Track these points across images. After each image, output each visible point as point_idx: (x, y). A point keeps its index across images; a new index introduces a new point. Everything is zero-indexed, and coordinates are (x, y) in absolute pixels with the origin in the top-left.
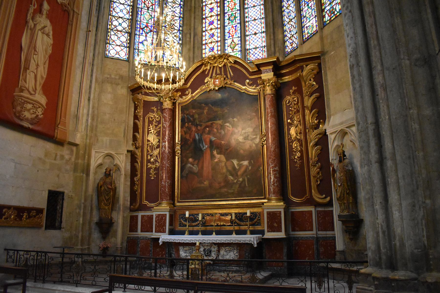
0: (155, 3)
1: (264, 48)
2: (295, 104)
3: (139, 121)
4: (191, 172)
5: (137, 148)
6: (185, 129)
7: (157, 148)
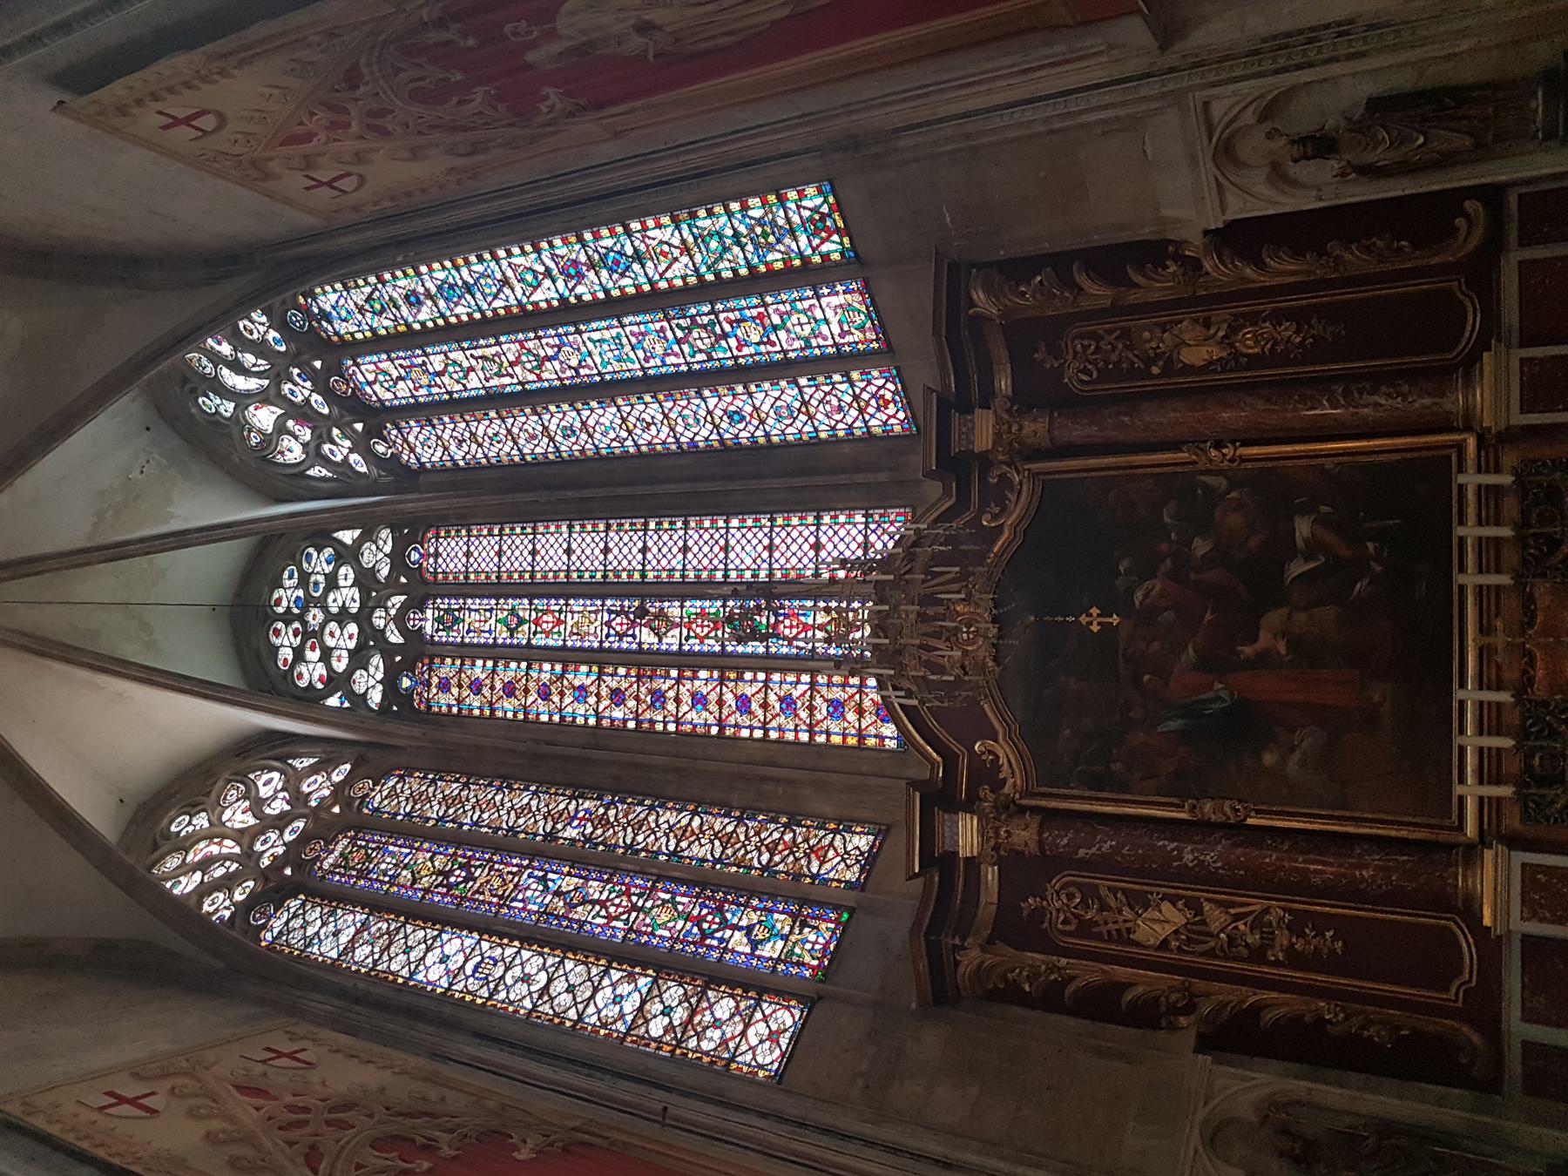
0: (623, 884)
1: (872, 516)
2: (1098, 350)
3: (1073, 978)
5: (1190, 1009)
7: (1199, 911)
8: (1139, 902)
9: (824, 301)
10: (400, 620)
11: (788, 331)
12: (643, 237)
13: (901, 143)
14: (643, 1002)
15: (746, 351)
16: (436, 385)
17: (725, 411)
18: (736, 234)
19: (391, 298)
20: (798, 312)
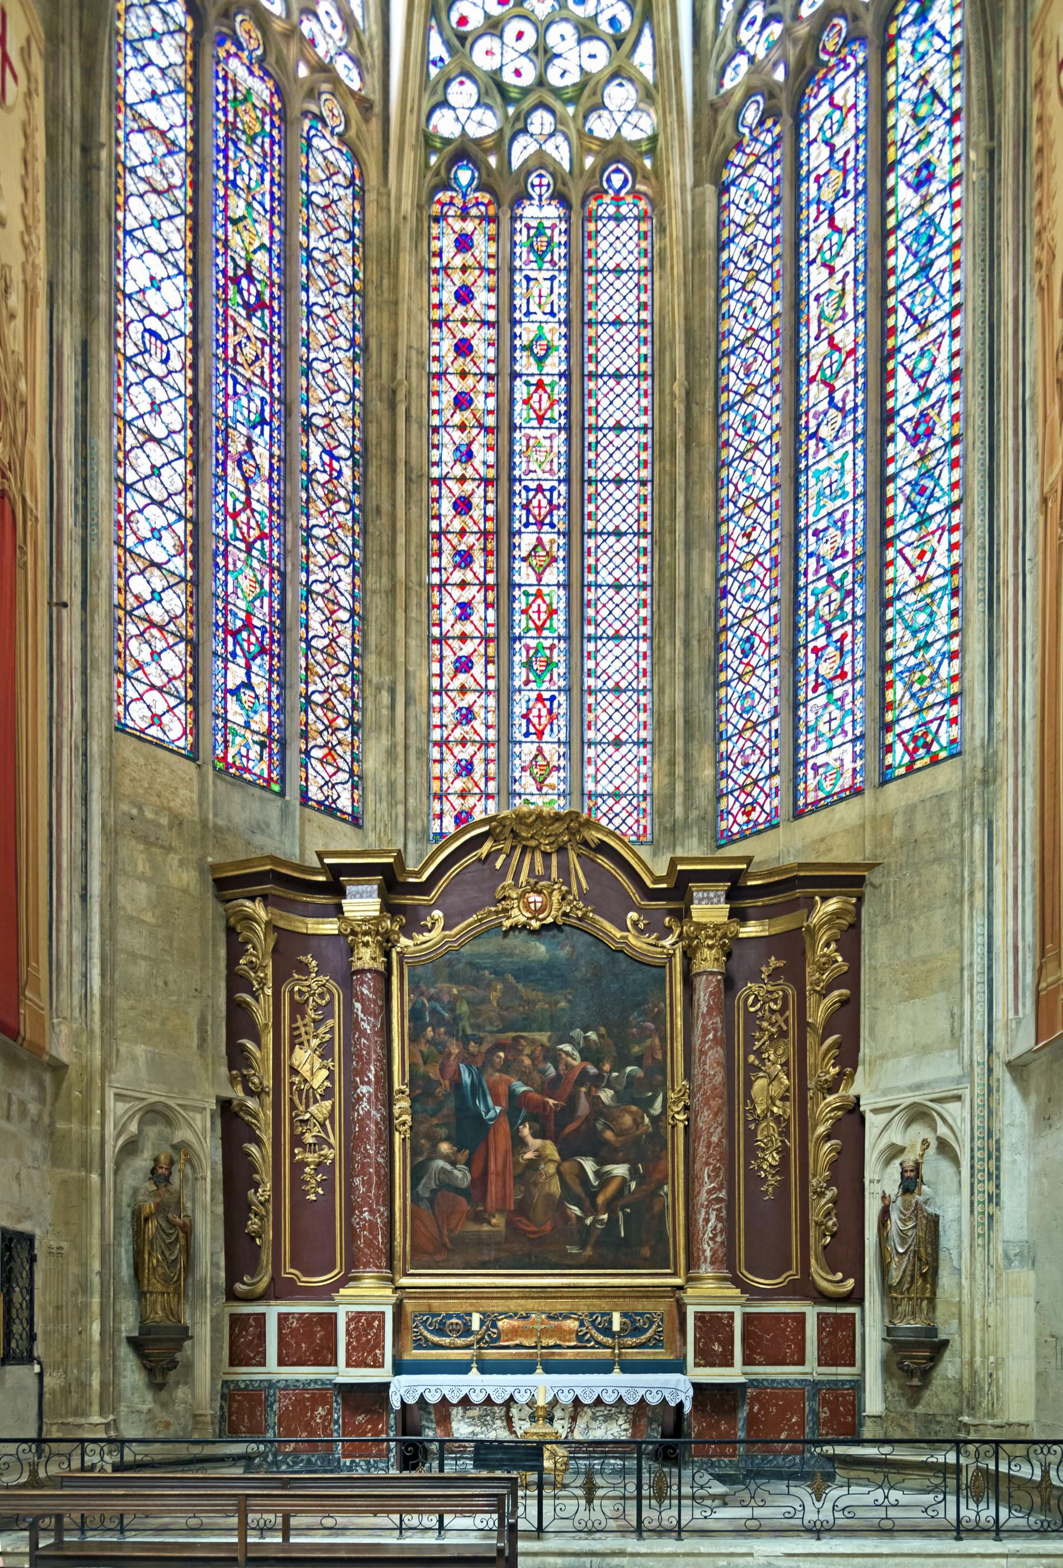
2: (772, 1011)
4: (446, 1185)
6: (424, 1048)
7: (324, 1097)
8: (325, 1051)
9: (849, 746)
10: (541, 161)
11: (826, 706)
12: (943, 529)
13: (977, 829)
14: (159, 566)
15: (812, 657)
16: (819, 213)
17: (754, 633)
18: (927, 645)
19: (930, 135)
20: (843, 717)
